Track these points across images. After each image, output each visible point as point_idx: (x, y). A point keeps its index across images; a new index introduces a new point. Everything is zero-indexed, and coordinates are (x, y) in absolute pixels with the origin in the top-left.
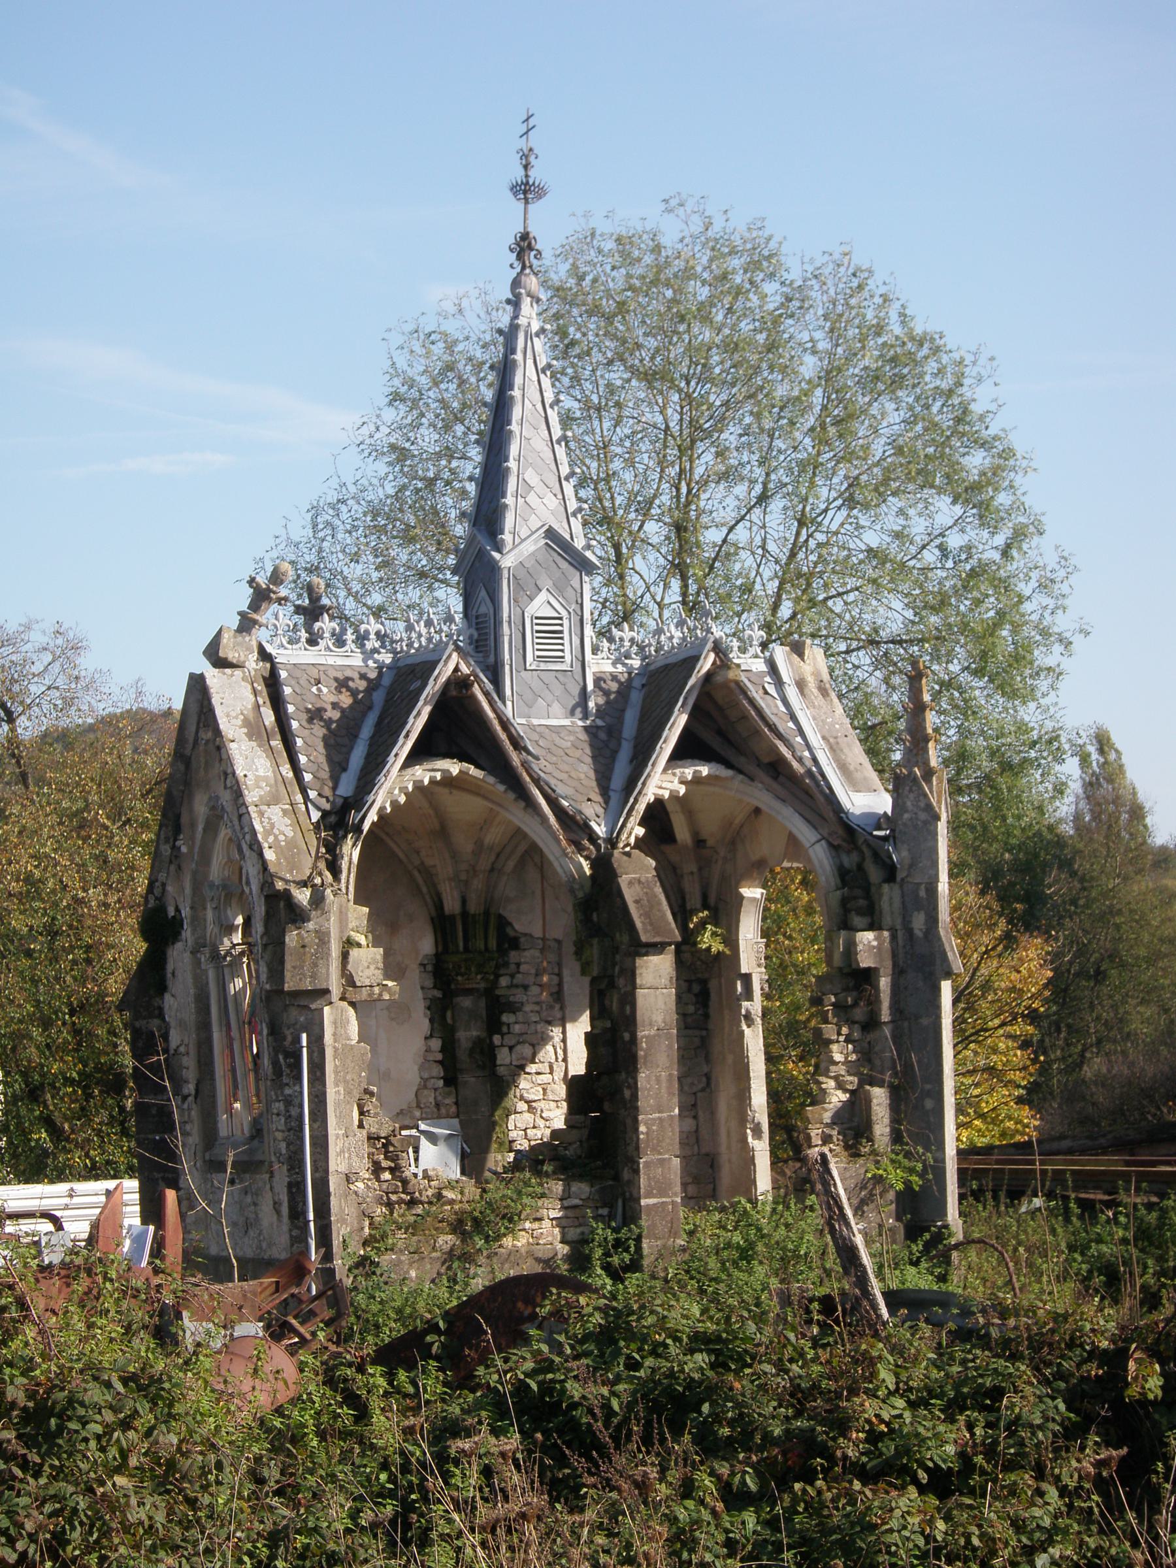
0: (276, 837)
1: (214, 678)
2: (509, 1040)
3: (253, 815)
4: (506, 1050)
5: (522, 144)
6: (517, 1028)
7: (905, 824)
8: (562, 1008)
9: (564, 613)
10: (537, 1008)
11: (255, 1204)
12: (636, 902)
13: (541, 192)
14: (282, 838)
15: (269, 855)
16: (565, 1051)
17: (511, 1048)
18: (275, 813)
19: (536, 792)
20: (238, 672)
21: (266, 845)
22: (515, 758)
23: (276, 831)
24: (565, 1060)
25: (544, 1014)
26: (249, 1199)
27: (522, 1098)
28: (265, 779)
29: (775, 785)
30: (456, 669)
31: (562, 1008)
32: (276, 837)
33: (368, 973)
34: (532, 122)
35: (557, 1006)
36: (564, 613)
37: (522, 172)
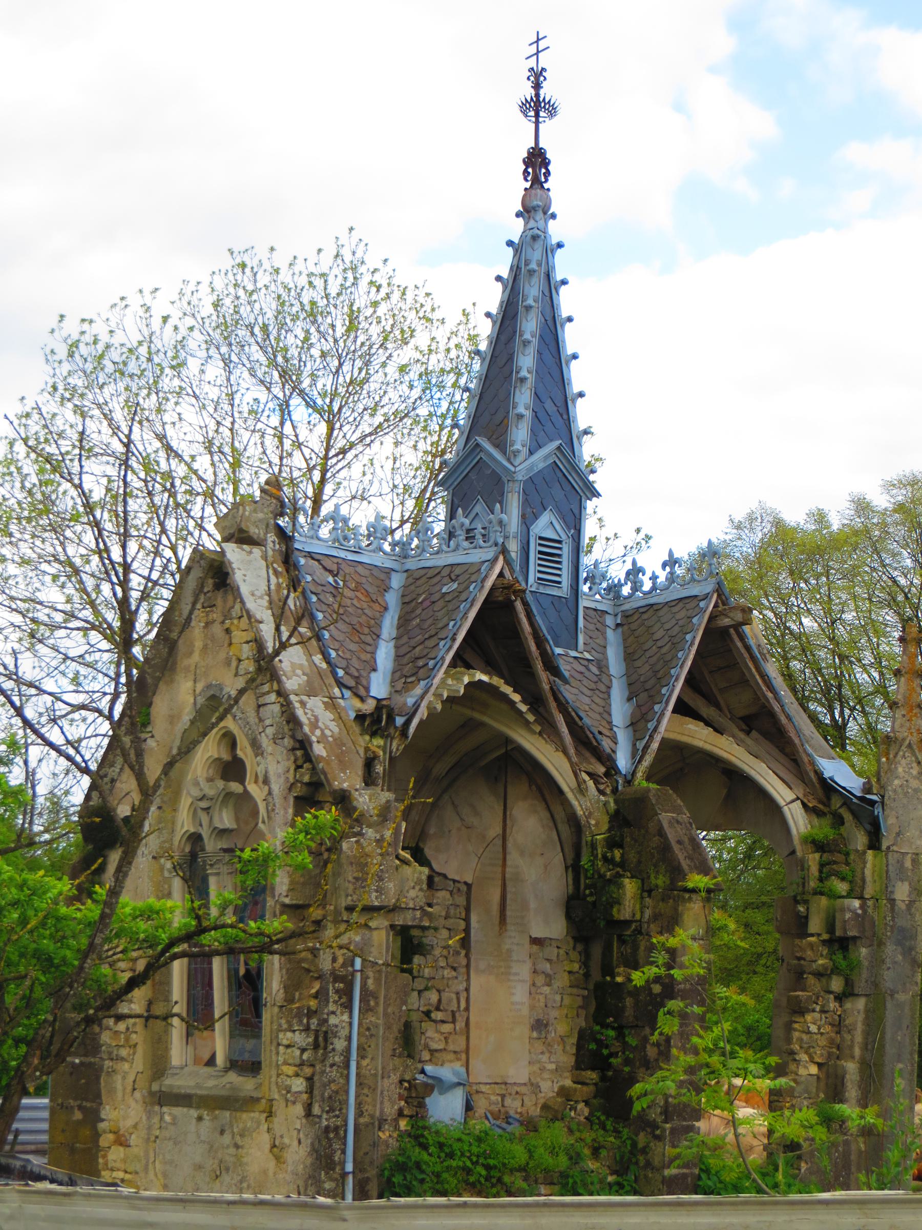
0: (322, 731)
1: (234, 554)
2: (419, 984)
3: (297, 705)
4: (415, 994)
5: (532, 63)
6: (427, 972)
7: (895, 791)
8: (467, 956)
9: (564, 537)
10: (445, 952)
11: (237, 1146)
12: (679, 842)
13: (552, 111)
14: (328, 733)
15: (319, 750)
16: (468, 1000)
17: (420, 992)
18: (316, 704)
19: (560, 719)
20: (257, 551)
21: (314, 739)
22: (544, 676)
23: (320, 724)
24: (467, 1009)
25: (451, 960)
26: (227, 1139)
27: (426, 1046)
28: (301, 667)
29: (748, 741)
30: (501, 575)
31: (467, 956)
32: (322, 731)
33: (412, 894)
34: (542, 45)
35: (463, 952)
36: (564, 537)
37: (533, 92)
